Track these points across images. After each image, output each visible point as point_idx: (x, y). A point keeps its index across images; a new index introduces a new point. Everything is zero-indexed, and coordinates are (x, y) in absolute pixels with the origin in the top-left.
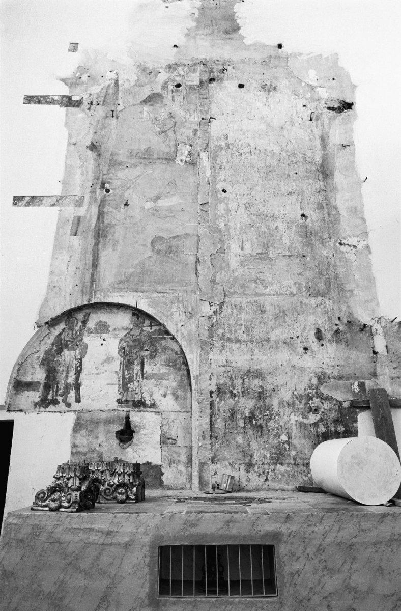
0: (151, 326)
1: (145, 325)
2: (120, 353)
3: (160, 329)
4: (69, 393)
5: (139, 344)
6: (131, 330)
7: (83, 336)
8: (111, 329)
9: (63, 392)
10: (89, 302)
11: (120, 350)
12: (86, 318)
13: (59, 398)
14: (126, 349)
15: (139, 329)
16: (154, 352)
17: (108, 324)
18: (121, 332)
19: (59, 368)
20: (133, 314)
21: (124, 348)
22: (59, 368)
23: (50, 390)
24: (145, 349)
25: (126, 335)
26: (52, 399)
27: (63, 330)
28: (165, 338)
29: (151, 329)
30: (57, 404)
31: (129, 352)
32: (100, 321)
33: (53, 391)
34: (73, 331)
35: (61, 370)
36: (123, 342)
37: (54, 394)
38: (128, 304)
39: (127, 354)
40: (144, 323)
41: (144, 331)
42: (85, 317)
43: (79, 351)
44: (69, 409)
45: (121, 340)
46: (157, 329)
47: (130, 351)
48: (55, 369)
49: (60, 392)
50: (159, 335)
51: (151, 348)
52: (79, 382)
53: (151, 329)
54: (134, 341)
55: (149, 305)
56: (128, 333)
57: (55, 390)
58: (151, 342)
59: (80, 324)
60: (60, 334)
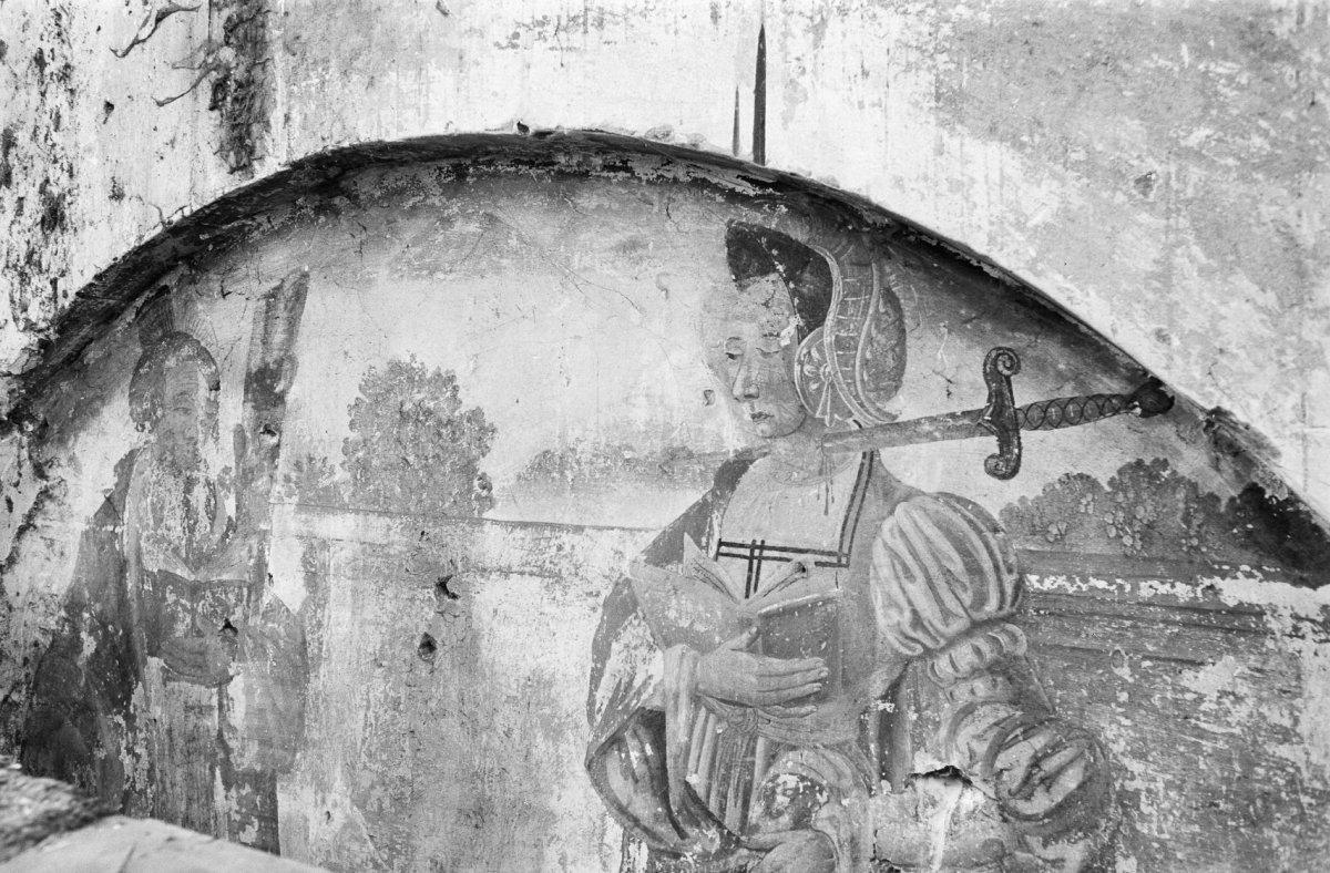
0: (1003, 422)
1: (905, 406)
2: (617, 782)
3: (1143, 474)
5: (841, 681)
6: (731, 473)
7: (264, 535)
8: (499, 466)
10: (240, 144)
11: (616, 741)
12: (278, 337)
14: (676, 729)
15: (825, 471)
16: (1061, 822)
17: (468, 403)
18: (611, 510)
20: (747, 255)
21: (655, 723)
24: (924, 762)
25: (666, 551)
27: (126, 465)
28: (1243, 624)
29: (1006, 466)
31: (720, 767)
32: (396, 368)
34: (190, 484)
36: (634, 632)
38: (633, 123)
39: (697, 810)
40: (890, 378)
41: (893, 495)
42: (269, 315)
45: (621, 606)
46: (1104, 468)
47: (729, 764)
50: (1137, 565)
51: (1018, 756)
53: (1006, 466)
54: (771, 635)
55: (949, 102)
56: (696, 521)
58: (1001, 668)
59: (235, 409)
60: (111, 508)
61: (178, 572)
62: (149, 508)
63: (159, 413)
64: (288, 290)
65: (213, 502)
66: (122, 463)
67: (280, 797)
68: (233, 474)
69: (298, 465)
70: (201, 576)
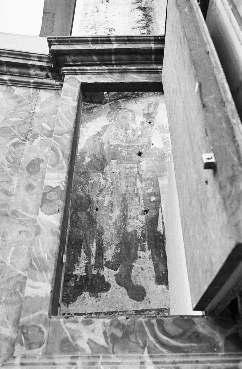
4: (135, 258)
9: (117, 256)
13: (109, 275)
19: (100, 198)
22: (100, 198)
23: (80, 252)
26: (87, 276)
30: (102, 290)
33: (88, 254)
34: (126, 130)
35: (106, 203)
37: (93, 260)
43: (147, 163)
44: (141, 306)
48: (90, 202)
49: (109, 255)
52: (160, 228)
57: (93, 251)
61: (123, 144)
62: (113, 134)
63: (116, 119)
64: (154, 103)
65: (134, 132)
66: (103, 127)
67: (159, 181)
68: (140, 128)
69: (159, 127)
70: (131, 144)
